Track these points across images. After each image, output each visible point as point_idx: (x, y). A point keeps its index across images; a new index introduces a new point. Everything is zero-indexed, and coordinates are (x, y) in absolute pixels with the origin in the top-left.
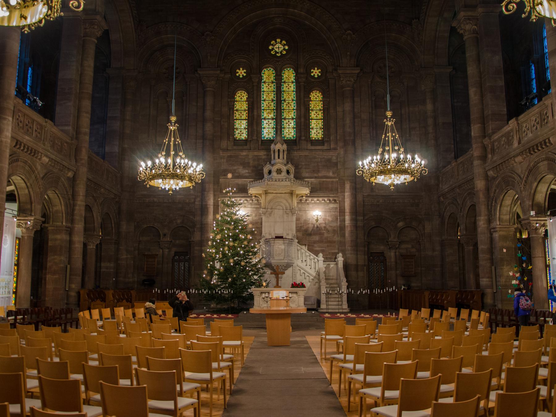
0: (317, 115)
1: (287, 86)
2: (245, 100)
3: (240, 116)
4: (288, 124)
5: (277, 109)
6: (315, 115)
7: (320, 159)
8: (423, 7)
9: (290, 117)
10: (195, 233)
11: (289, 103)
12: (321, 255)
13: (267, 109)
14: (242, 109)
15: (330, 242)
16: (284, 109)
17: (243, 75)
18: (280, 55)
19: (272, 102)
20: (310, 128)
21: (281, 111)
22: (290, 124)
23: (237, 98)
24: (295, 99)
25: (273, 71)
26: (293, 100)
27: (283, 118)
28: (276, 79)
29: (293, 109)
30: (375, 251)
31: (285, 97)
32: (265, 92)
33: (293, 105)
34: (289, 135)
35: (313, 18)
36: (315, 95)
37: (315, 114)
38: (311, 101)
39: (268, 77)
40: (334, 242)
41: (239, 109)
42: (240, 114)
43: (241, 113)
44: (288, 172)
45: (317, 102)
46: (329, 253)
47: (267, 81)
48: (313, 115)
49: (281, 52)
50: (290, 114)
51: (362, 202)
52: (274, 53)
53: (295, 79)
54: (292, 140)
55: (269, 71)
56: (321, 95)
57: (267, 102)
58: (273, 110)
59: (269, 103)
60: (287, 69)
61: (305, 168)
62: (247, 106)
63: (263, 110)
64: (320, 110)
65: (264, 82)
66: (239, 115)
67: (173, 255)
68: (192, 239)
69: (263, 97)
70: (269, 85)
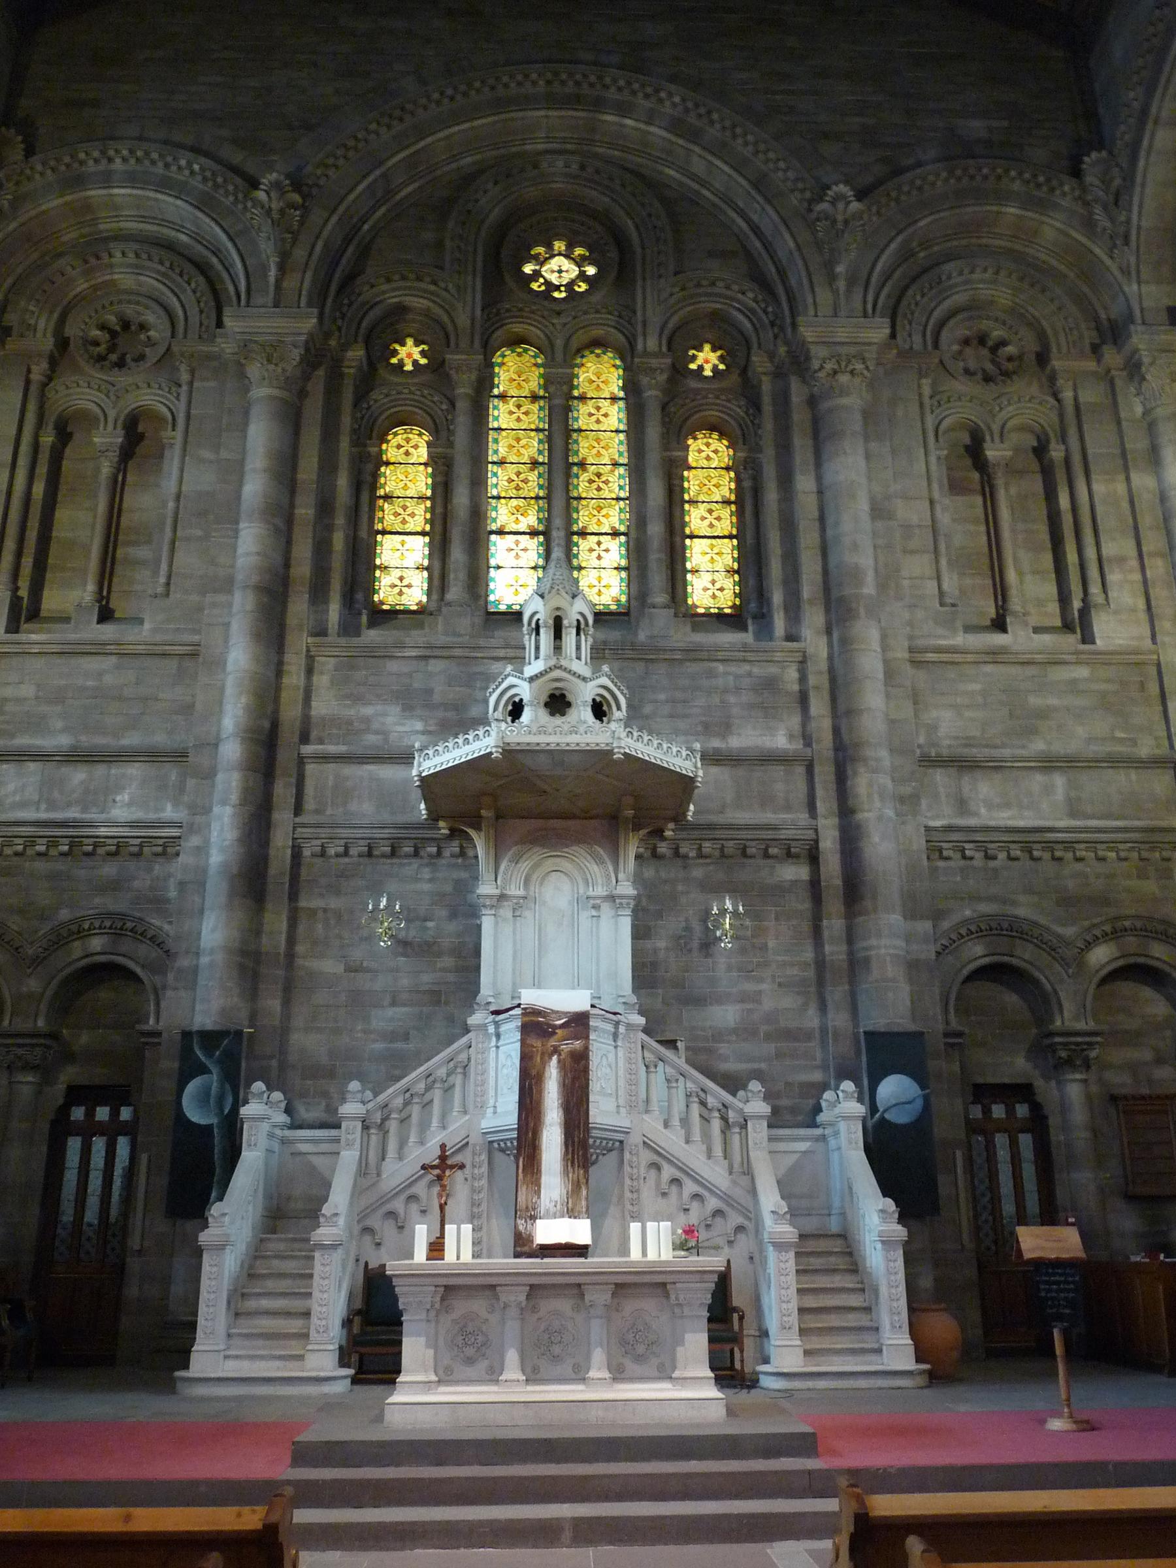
0: (715, 522)
1: (593, 411)
2: (423, 460)
3: (400, 518)
4: (595, 554)
5: (548, 498)
6: (707, 522)
7: (731, 678)
8: (1132, 94)
9: (606, 529)
10: (169, 993)
11: (599, 475)
12: (755, 1086)
13: (512, 493)
14: (409, 493)
15: (789, 1035)
16: (580, 498)
17: (415, 363)
18: (563, 295)
19: (532, 470)
20: (685, 571)
21: (568, 505)
22: (603, 554)
23: (391, 452)
24: (624, 460)
25: (535, 357)
26: (615, 464)
27: (575, 529)
28: (546, 387)
29: (618, 499)
30: (991, 1080)
31: (583, 452)
32: (504, 433)
33: (617, 483)
34: (599, 593)
35: (697, 149)
36: (704, 448)
37: (703, 518)
38: (690, 468)
39: (515, 377)
40: (808, 1036)
41: (397, 493)
42: (400, 511)
43: (405, 508)
44: (599, 710)
45: (713, 473)
46: (787, 1084)
47: (511, 393)
48: (696, 518)
49: (570, 286)
50: (606, 516)
51: (925, 862)
52: (543, 288)
53: (624, 388)
54: (611, 613)
55: (519, 355)
56: (728, 447)
57: (511, 470)
58: (537, 498)
59: (518, 474)
60: (592, 352)
61: (671, 716)
62: (430, 481)
63: (493, 498)
64: (727, 502)
65: (503, 397)
66: (396, 514)
67: (61, 1101)
68: (152, 1021)
69: (496, 452)
70: (519, 407)
